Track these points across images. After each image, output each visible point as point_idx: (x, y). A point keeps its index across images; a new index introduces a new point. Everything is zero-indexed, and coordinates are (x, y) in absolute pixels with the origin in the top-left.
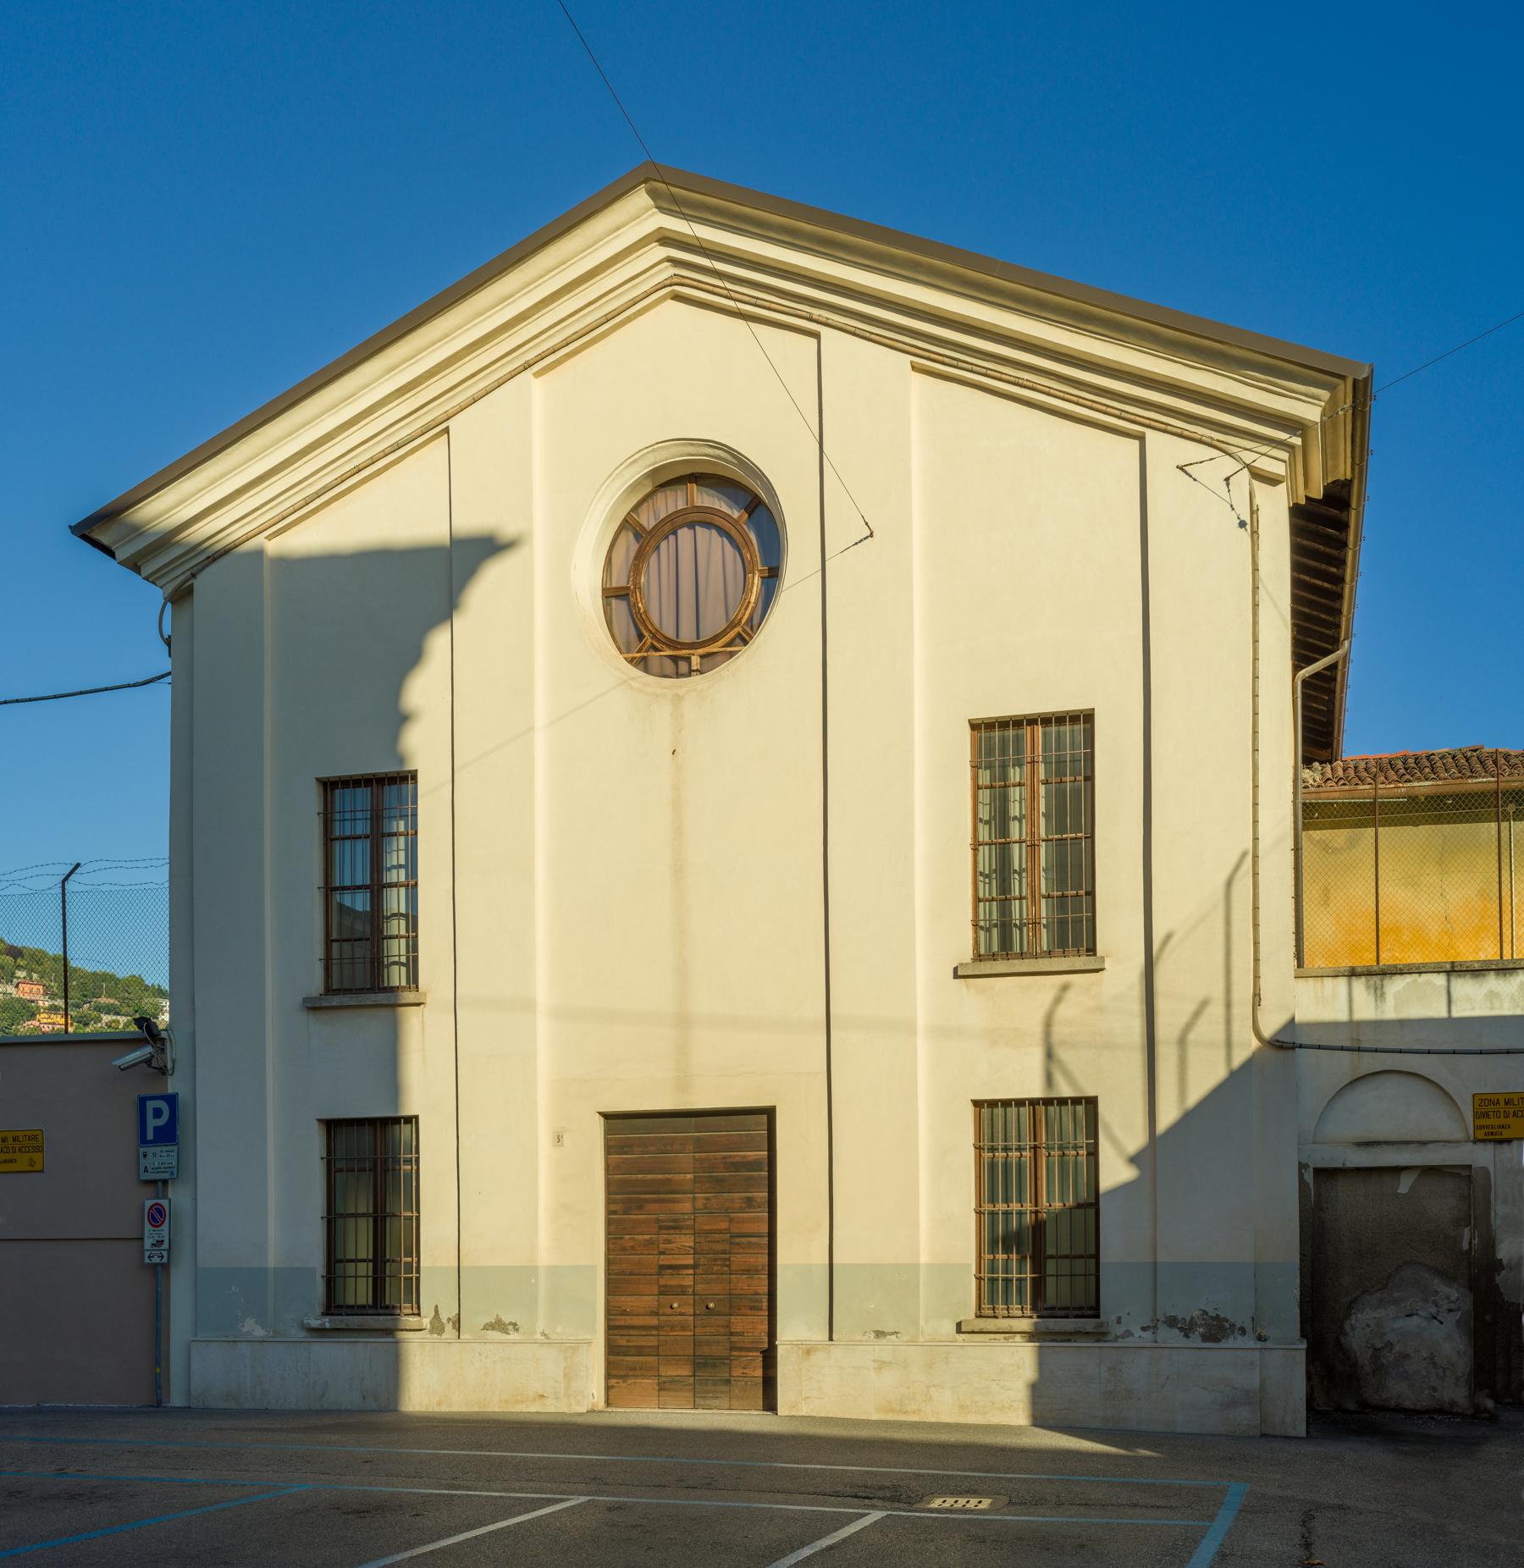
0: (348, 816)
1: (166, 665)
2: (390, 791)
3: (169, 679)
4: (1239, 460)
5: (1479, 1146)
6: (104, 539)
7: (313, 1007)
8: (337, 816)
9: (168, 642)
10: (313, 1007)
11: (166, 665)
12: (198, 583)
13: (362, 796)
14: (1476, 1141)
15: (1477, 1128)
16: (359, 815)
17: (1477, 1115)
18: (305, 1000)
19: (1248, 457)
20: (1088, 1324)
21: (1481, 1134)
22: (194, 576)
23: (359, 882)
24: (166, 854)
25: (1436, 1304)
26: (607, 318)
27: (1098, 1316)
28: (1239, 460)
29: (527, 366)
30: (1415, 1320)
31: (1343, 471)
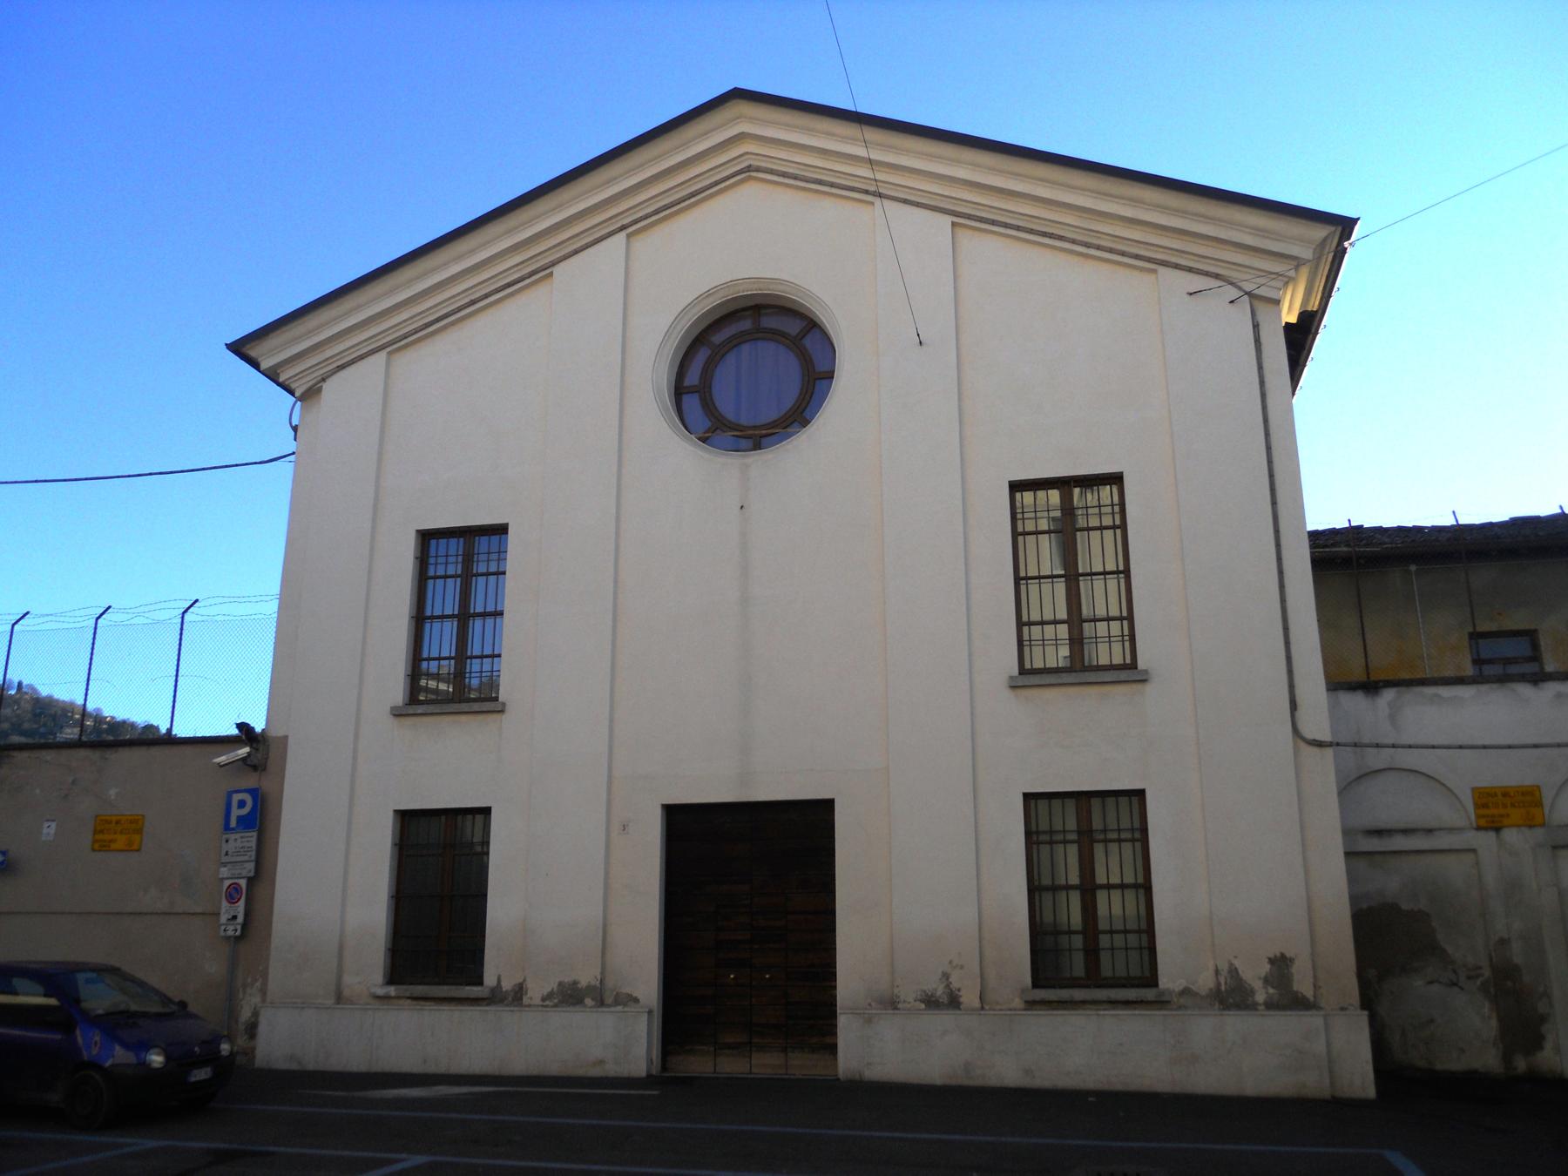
0: (441, 560)
1: (291, 446)
2: (482, 543)
3: (292, 458)
4: (1240, 288)
5: (1481, 834)
6: (253, 353)
7: (398, 713)
8: (432, 560)
9: (295, 429)
10: (398, 713)
11: (291, 446)
12: (326, 386)
13: (455, 545)
14: (1479, 828)
15: (1478, 817)
16: (451, 559)
17: (1477, 806)
18: (393, 708)
19: (1248, 287)
20: (1149, 994)
21: (1483, 822)
22: (324, 380)
23: (448, 612)
24: (275, 588)
25: (1455, 971)
26: (693, 195)
27: (1156, 985)
28: (1240, 288)
29: (623, 228)
30: (1435, 988)
31: (1314, 305)
